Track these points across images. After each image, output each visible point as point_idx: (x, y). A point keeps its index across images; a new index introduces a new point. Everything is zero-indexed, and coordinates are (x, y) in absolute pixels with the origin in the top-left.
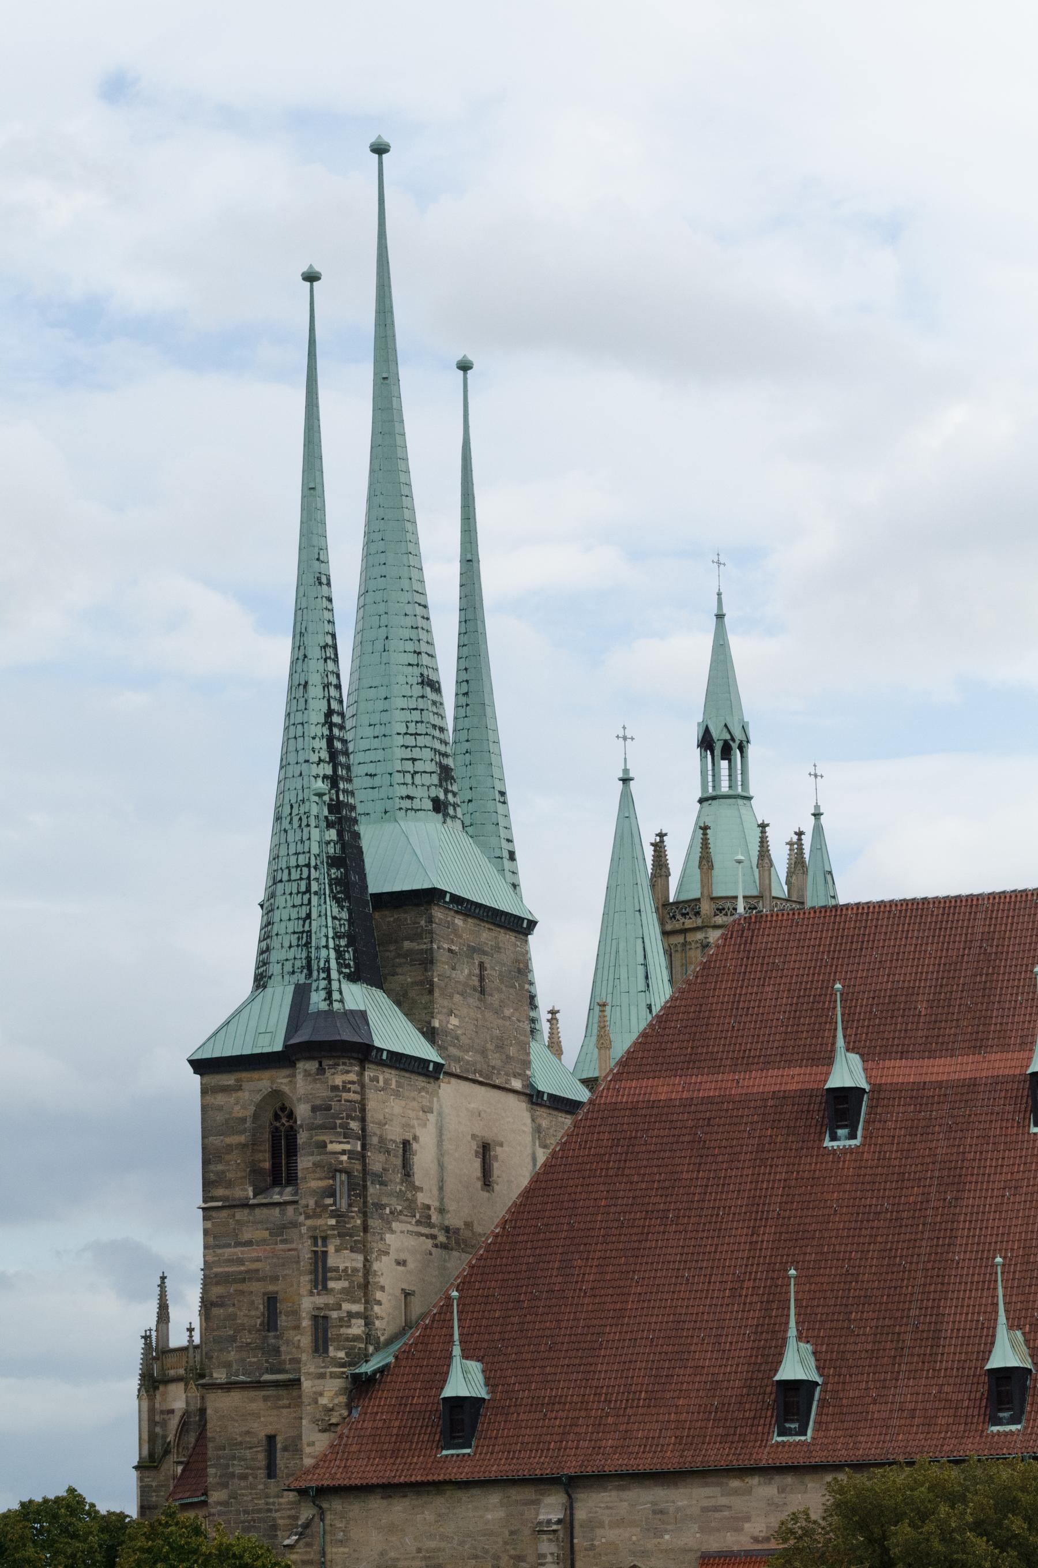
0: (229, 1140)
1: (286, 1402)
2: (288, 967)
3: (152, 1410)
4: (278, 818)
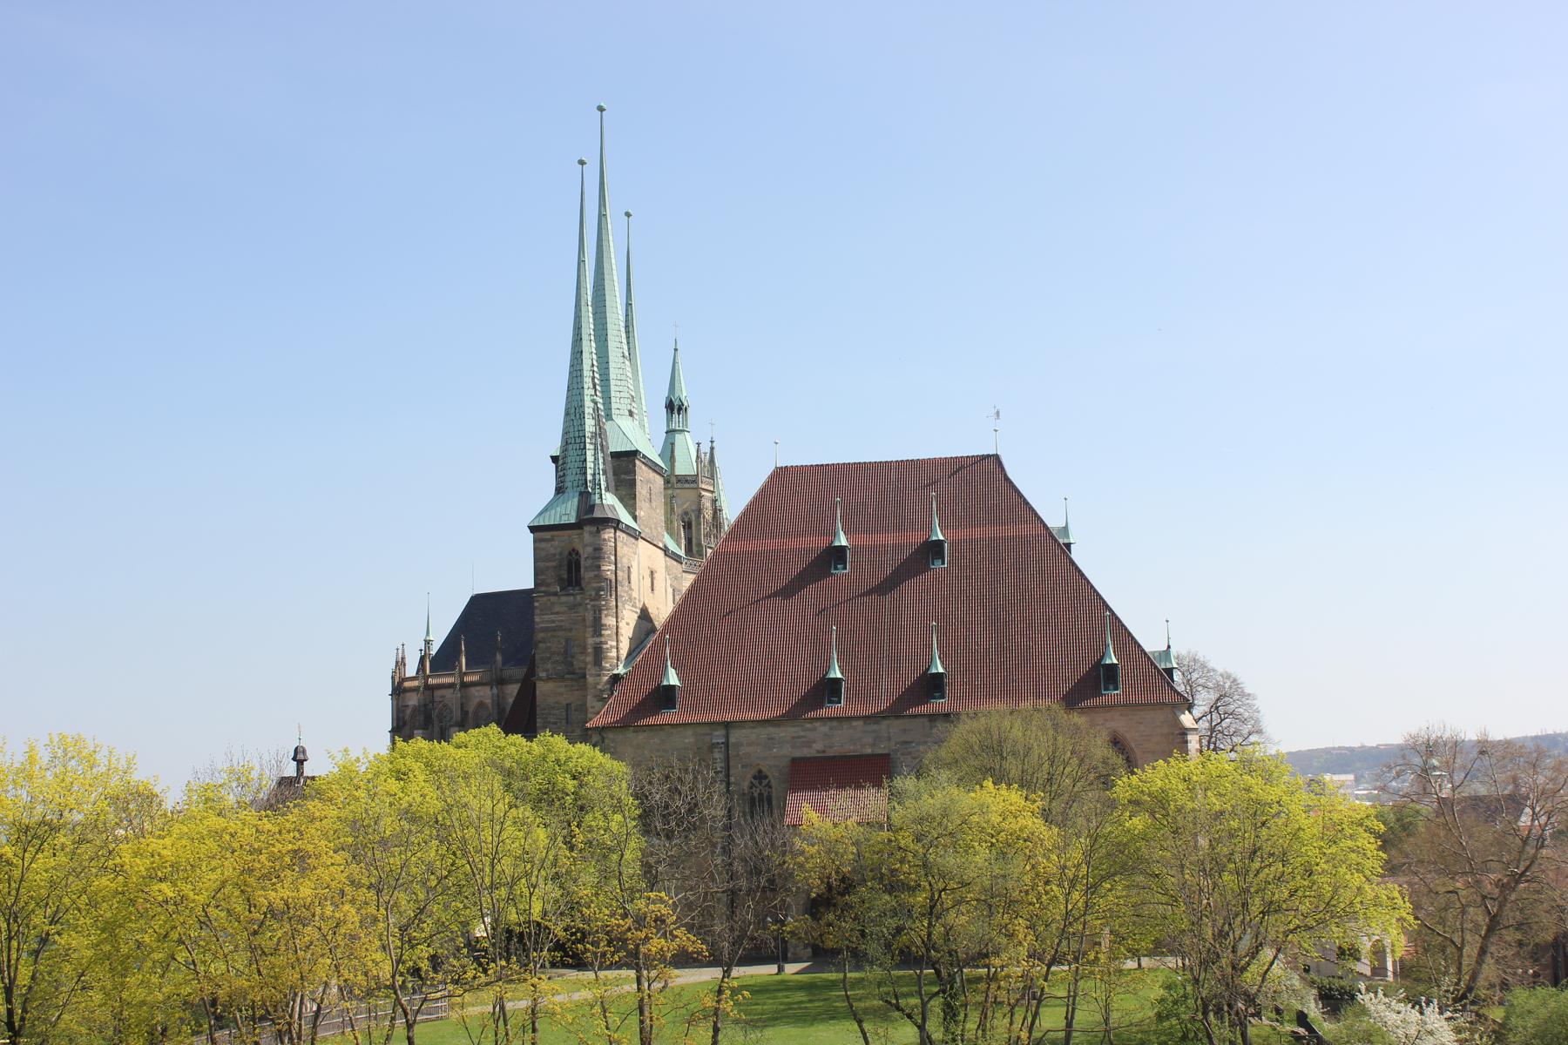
0: (548, 564)
1: (576, 688)
2: (575, 484)
3: (397, 705)
4: (567, 414)
